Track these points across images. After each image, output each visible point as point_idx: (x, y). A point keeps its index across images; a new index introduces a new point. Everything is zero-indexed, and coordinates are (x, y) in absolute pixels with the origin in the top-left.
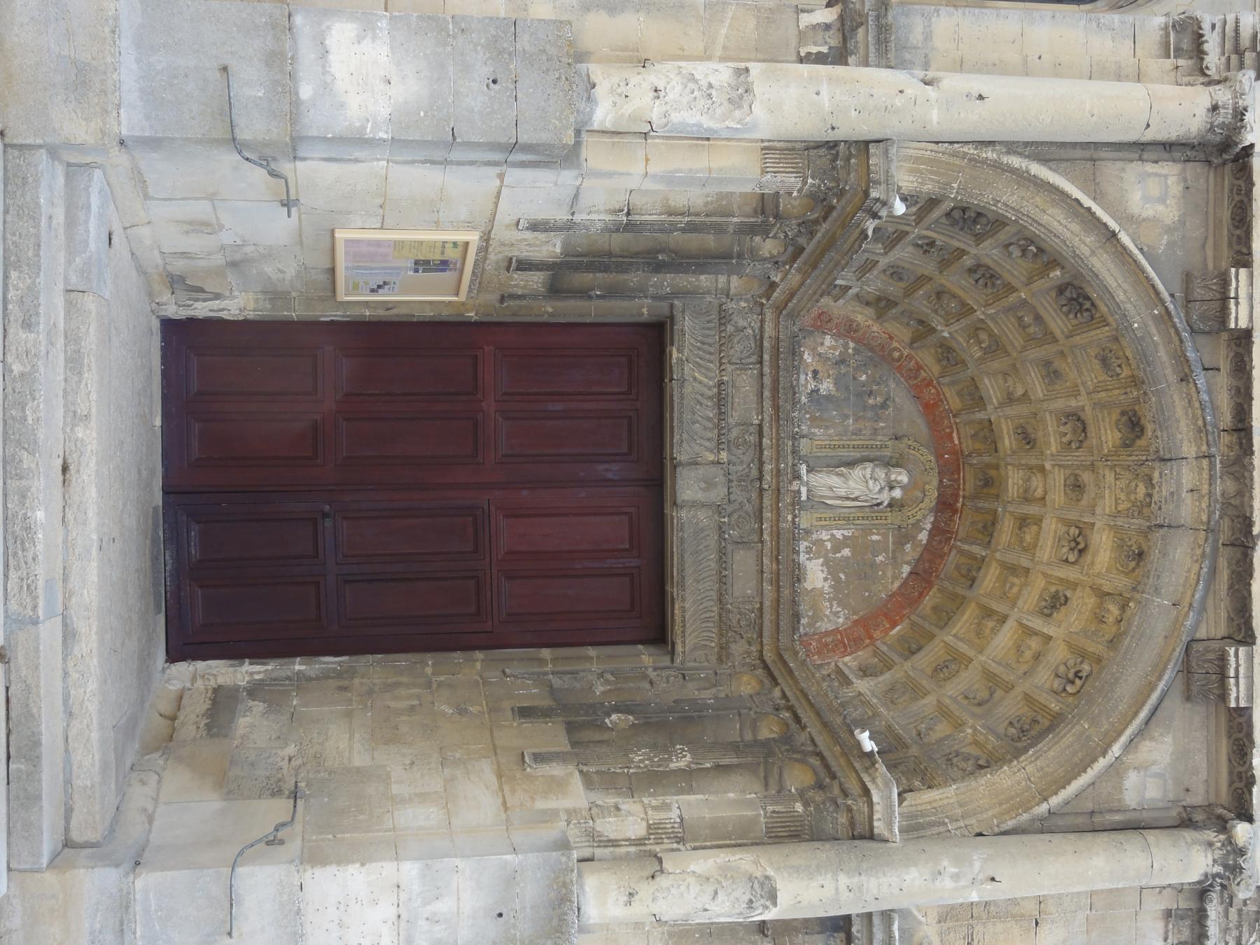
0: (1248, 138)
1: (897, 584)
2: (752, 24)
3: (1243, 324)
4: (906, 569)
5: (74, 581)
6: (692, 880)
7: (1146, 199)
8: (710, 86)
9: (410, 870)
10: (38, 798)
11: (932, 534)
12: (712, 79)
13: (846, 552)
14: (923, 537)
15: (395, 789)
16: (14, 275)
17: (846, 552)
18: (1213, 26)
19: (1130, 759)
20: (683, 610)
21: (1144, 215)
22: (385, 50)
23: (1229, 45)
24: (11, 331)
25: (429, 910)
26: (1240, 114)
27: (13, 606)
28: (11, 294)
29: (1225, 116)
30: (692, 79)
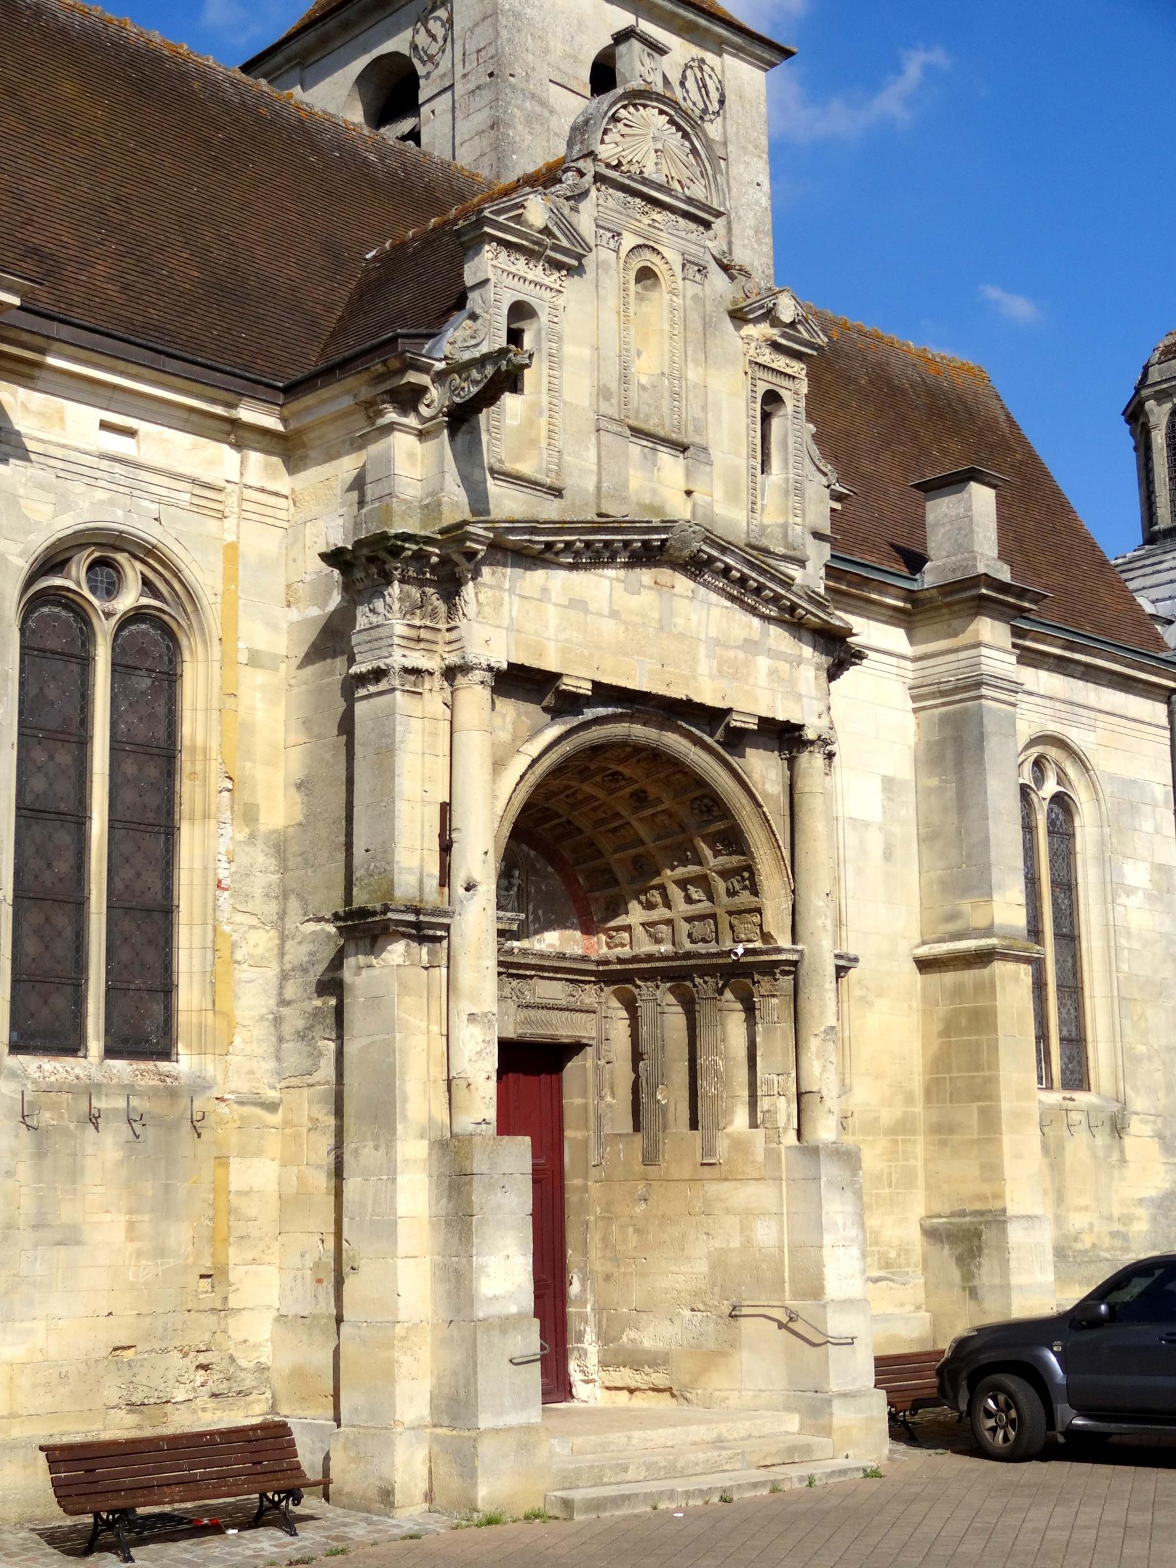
0: (505, 666)
1: (557, 877)
2: (407, 999)
3: (589, 686)
4: (550, 869)
5: (697, 1439)
6: (825, 1076)
7: (503, 728)
8: (484, 1041)
9: (828, 1239)
10: (809, 1445)
11: (530, 846)
12: (480, 1040)
13: (540, 912)
14: (532, 853)
15: (735, 1244)
16: (605, 1480)
17: (540, 912)
18: (404, 656)
19: (759, 787)
20: (567, 1037)
21: (511, 731)
22: (492, 1259)
23: (412, 645)
24: (628, 1479)
25: (841, 1229)
26: (490, 669)
27: (738, 1466)
28: (613, 1480)
29: (488, 676)
30: (479, 1053)
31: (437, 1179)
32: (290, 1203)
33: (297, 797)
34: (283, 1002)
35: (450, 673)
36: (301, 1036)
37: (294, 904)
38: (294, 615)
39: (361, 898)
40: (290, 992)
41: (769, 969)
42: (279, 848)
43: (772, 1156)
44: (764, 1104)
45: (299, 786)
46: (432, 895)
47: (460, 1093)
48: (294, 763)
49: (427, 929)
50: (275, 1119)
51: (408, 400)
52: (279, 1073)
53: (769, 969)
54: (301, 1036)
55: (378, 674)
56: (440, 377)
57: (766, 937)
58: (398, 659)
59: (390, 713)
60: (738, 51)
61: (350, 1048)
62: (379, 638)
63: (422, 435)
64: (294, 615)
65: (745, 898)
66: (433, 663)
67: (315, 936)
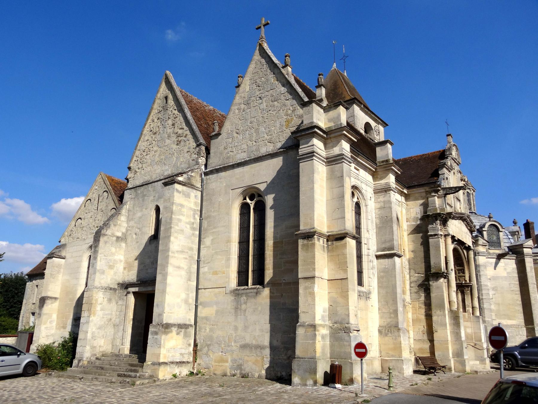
31: (450, 317)
32: (415, 321)
33: (412, 253)
34: (410, 287)
35: (445, 236)
36: (416, 293)
37: (412, 271)
38: (409, 223)
39: (433, 271)
40: (412, 285)
41: (468, 286)
42: (409, 261)
43: (469, 317)
44: (467, 309)
45: (412, 251)
46: (445, 271)
47: (452, 304)
48: (411, 247)
49: (446, 276)
50: (411, 306)
51: (437, 191)
52: (411, 299)
53: (468, 286)
54: (416, 293)
55: (435, 235)
56: (444, 189)
57: (466, 281)
58: (440, 233)
59: (439, 241)
60: (381, 125)
61: (433, 295)
62: (434, 229)
63: (438, 197)
64: (409, 223)
65: (461, 274)
66: (442, 234)
67: (419, 277)
